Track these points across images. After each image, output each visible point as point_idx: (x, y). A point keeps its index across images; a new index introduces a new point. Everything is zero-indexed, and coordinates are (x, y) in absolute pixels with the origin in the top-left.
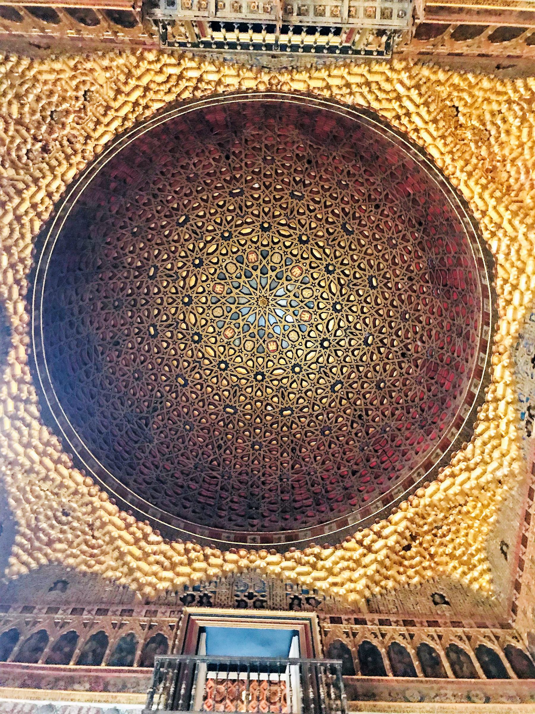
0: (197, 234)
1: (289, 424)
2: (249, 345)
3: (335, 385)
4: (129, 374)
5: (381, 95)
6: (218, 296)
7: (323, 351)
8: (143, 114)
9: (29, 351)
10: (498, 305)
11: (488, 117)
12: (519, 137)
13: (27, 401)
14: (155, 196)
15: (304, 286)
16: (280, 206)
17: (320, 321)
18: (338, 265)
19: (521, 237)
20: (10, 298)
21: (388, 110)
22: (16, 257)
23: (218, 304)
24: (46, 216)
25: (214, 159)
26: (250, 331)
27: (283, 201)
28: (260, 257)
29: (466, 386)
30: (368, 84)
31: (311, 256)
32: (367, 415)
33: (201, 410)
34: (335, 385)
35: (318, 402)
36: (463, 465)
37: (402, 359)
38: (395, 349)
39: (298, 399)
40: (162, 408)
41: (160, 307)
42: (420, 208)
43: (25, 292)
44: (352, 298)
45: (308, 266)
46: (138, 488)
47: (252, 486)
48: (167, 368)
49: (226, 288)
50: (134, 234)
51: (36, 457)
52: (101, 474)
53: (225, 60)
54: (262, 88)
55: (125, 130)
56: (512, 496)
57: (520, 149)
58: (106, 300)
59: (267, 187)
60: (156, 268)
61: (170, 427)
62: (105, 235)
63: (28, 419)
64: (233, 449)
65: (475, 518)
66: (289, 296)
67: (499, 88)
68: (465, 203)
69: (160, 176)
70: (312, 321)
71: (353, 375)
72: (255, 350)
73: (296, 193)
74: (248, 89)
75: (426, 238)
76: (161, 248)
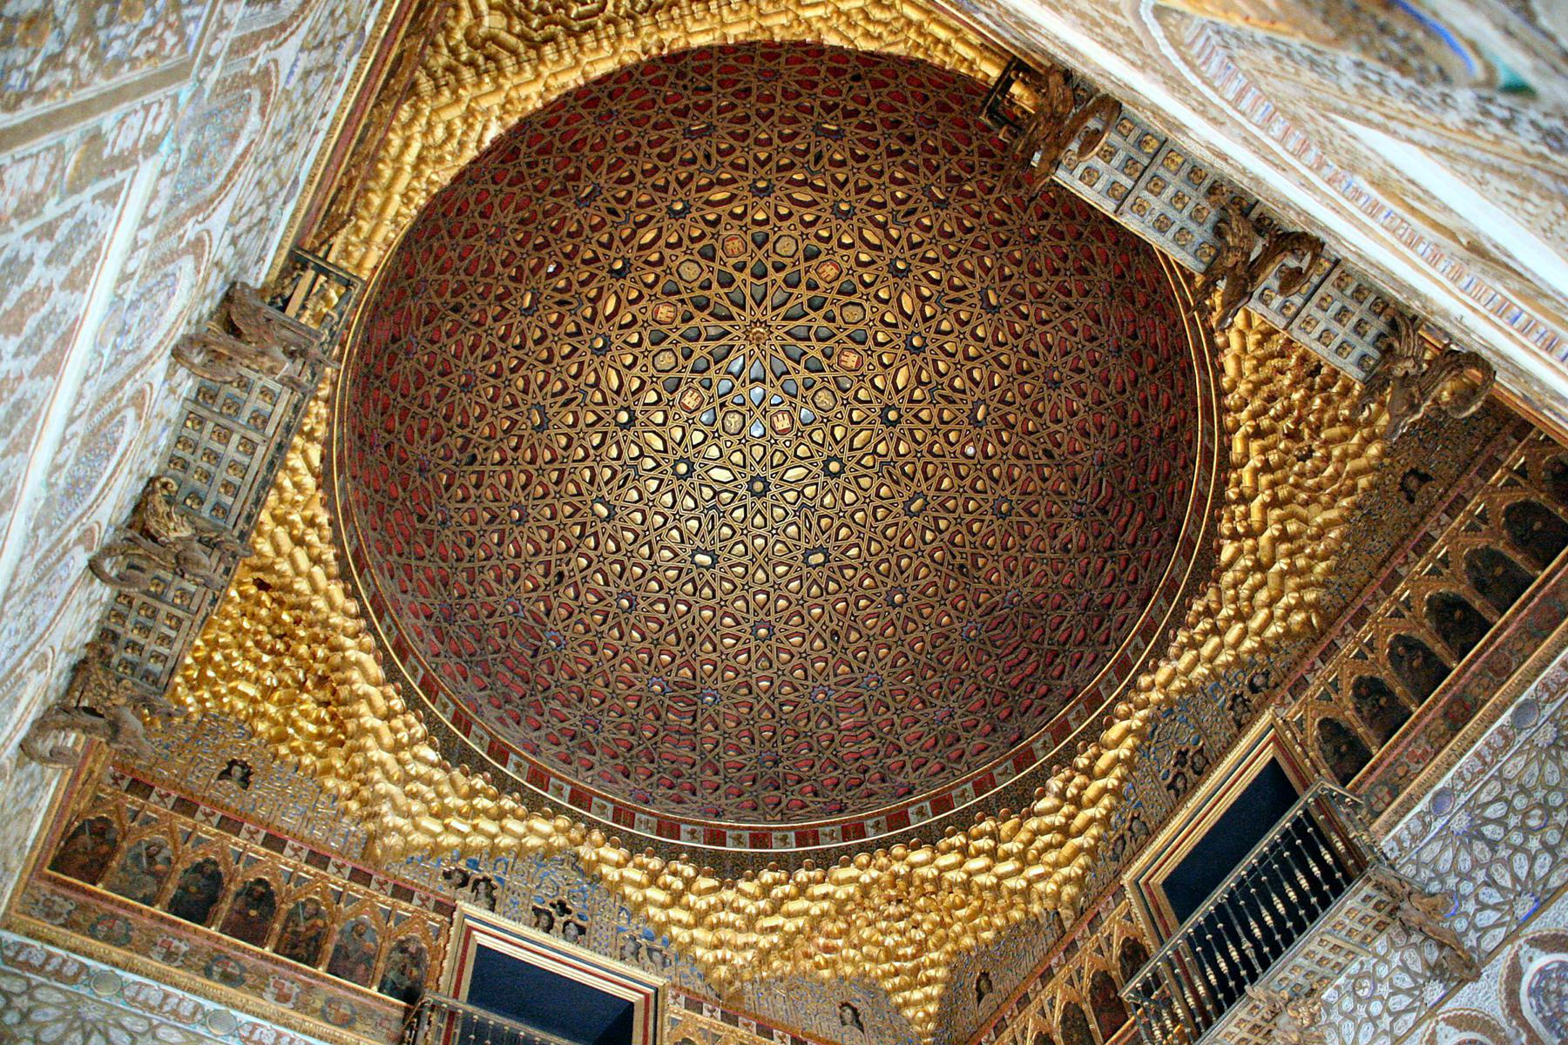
2: (690, 271)
5: (1041, 841)
10: (651, 855)
11: (918, 917)
12: (868, 941)
19: (752, 938)
21: (1015, 835)
23: (800, 254)
26: (715, 285)
29: (511, 736)
30: (1065, 831)
34: (543, 414)
35: (523, 371)
36: (404, 736)
45: (780, 446)
49: (822, 284)
55: (1227, 482)
56: (336, 819)
65: (287, 717)
67: (949, 947)
68: (825, 861)
70: (677, 409)
72: (676, 278)
73: (919, 502)
74: (1156, 668)
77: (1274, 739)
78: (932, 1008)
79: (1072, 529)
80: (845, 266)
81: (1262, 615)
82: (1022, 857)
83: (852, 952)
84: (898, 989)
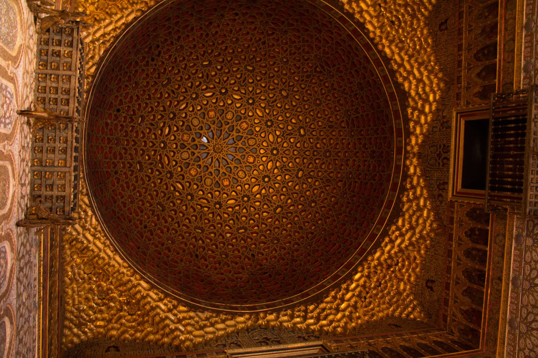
0: (266, 199)
1: (206, 54)
2: (229, 116)
3: (167, 84)
4: (324, 104)
6: (251, 154)
7: (174, 110)
8: (336, 293)
9: (408, 140)
12: (80, 296)
13: (414, 109)
14: (301, 228)
15: (187, 161)
16: (209, 221)
17: (176, 134)
18: (164, 178)
20: (419, 178)
22: (414, 204)
23: (251, 148)
24: (393, 228)
25: (263, 254)
26: (228, 126)
27: (209, 225)
28: (220, 182)
31: (184, 184)
32: (148, 62)
33: (272, 71)
34: (167, 84)
37: (120, 107)
38: (124, 115)
39: (196, 73)
40: (303, 77)
41: (295, 148)
42: (123, 231)
43: (409, 180)
44: (153, 153)
45: (185, 176)
46: (340, 30)
47: (247, 13)
48: (294, 104)
50: (314, 201)
51: (416, 72)
52: (369, 49)
53: (293, 332)
54: (262, 315)
57: (79, 289)
58: (336, 158)
59: (221, 234)
60: (297, 176)
61: (299, 63)
62: (337, 203)
63: (417, 98)
64: (253, 41)
66: (199, 153)
68: (116, 250)
69: (299, 242)
70: (181, 134)
71: (153, 91)
73: (200, 231)
74: (271, 314)
75: (113, 207)
76: (294, 191)
77: (320, 349)
78: (76, 340)
79: (244, 276)
80: (256, 163)
81: (324, 322)
82: (179, 321)
83: (76, 289)
84: (71, 321)
